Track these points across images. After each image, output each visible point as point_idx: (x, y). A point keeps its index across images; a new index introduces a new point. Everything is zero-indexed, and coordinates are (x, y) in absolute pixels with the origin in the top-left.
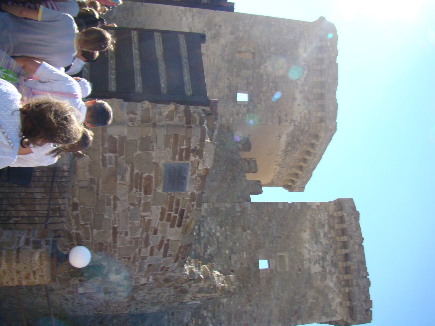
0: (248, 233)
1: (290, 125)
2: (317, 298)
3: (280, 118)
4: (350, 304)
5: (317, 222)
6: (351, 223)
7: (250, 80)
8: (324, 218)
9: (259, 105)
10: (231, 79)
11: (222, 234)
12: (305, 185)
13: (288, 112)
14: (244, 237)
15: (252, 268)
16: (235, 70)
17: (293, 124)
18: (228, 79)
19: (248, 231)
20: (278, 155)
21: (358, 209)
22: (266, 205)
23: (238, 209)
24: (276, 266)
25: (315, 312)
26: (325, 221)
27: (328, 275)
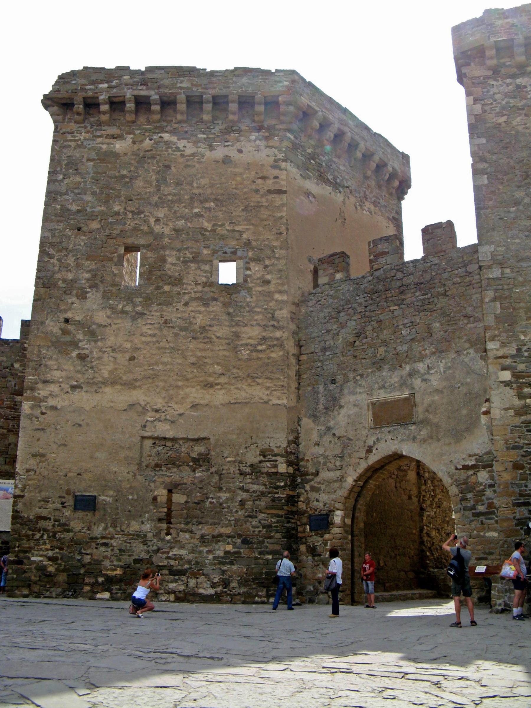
1: (286, 170)
3: (270, 192)
7: (189, 255)
9: (245, 236)
10: (186, 297)
12: (399, 152)
13: (257, 173)
16: (167, 288)
17: (283, 165)
18: (186, 304)
20: (344, 202)
21: (478, 14)
22: (482, 212)
23: (496, 273)
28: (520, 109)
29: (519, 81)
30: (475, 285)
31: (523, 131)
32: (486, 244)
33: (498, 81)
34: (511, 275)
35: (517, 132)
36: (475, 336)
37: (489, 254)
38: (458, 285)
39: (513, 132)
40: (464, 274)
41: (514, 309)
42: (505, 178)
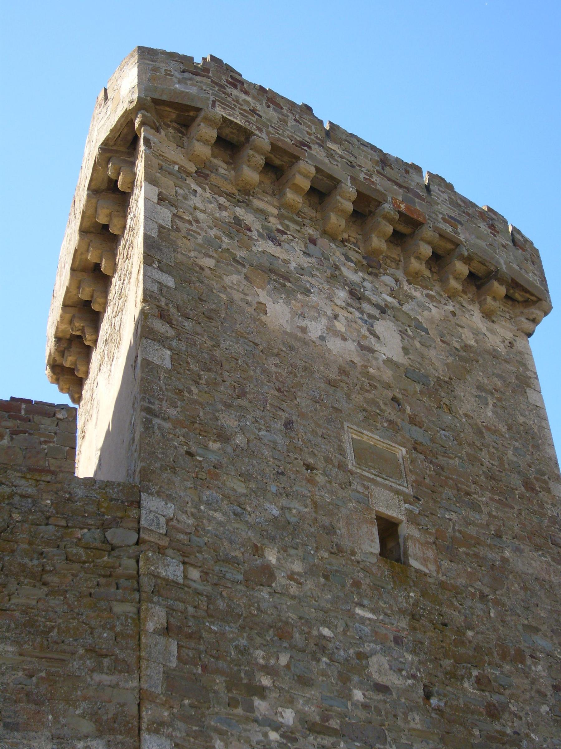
0: (278, 559)
2: (480, 387)
4: (501, 281)
5: (226, 240)
6: (254, 111)
8: (211, 203)
11: (290, 702)
14: (294, 590)
15: (411, 601)
19: (272, 557)
22: (156, 421)
24: (397, 492)
25: (521, 419)
26: (221, 207)
27: (405, 308)
28: (238, 262)
29: (240, 211)
30: (123, 582)
31: (240, 303)
32: (158, 494)
33: (204, 189)
34: (200, 587)
35: (231, 301)
36: (112, 710)
37: (162, 520)
38: (76, 566)
39: (224, 297)
40: (98, 544)
41: (205, 668)
42: (205, 376)
